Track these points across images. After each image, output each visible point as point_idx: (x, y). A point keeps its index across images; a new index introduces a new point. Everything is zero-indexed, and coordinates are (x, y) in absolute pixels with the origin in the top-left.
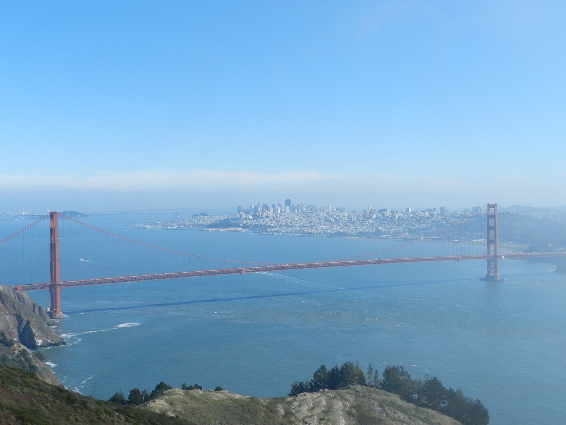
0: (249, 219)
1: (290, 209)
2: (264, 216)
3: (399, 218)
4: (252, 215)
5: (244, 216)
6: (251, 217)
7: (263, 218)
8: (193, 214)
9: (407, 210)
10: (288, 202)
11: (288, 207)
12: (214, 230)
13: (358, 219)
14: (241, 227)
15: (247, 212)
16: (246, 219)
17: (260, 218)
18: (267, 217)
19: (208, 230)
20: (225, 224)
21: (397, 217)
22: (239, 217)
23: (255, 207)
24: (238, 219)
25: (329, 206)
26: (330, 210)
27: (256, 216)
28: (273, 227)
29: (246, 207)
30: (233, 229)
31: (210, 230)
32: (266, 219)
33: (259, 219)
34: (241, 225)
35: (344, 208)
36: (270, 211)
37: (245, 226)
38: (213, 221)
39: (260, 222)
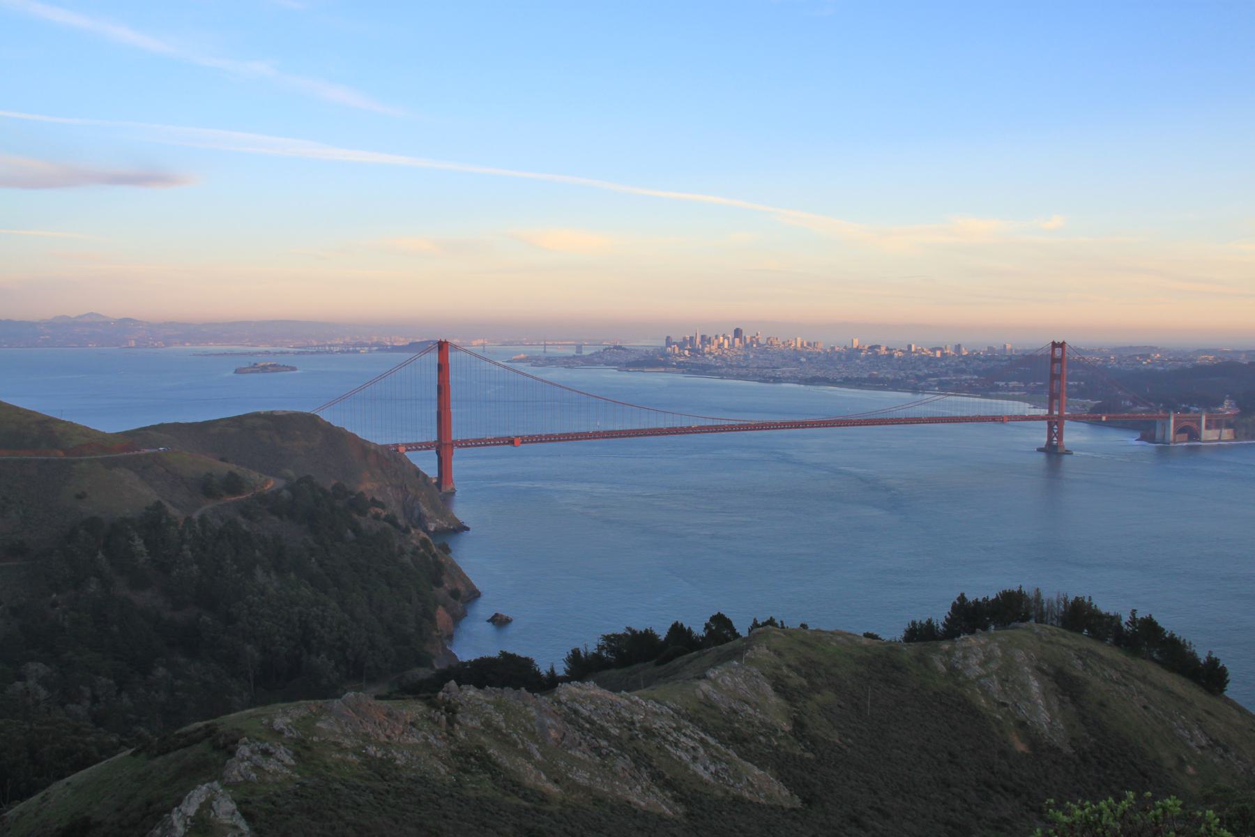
0: (685, 355)
1: (741, 342)
2: (705, 352)
4: (689, 350)
5: (677, 351)
6: (687, 352)
9: (910, 347)
10: (738, 333)
11: (737, 340)
14: (674, 366)
15: (681, 346)
16: (680, 356)
23: (691, 338)
25: (796, 339)
26: (799, 345)
29: (677, 338)
34: (675, 364)
35: (818, 343)
36: (713, 345)
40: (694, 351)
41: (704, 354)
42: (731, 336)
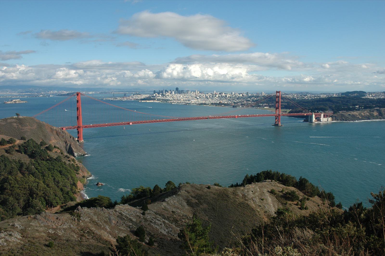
3: (229, 97)
4: (161, 95)
6: (160, 95)
7: (166, 96)
12: (144, 101)
13: (210, 97)
14: (156, 100)
16: (158, 97)
17: (165, 96)
18: (168, 96)
19: (141, 102)
21: (228, 96)
22: (155, 95)
24: (154, 96)
27: (163, 95)
28: (171, 100)
29: (157, 90)
30: (152, 101)
31: (142, 101)
32: (167, 96)
33: (164, 97)
34: (156, 99)
37: (158, 100)
38: (143, 97)
39: (164, 98)
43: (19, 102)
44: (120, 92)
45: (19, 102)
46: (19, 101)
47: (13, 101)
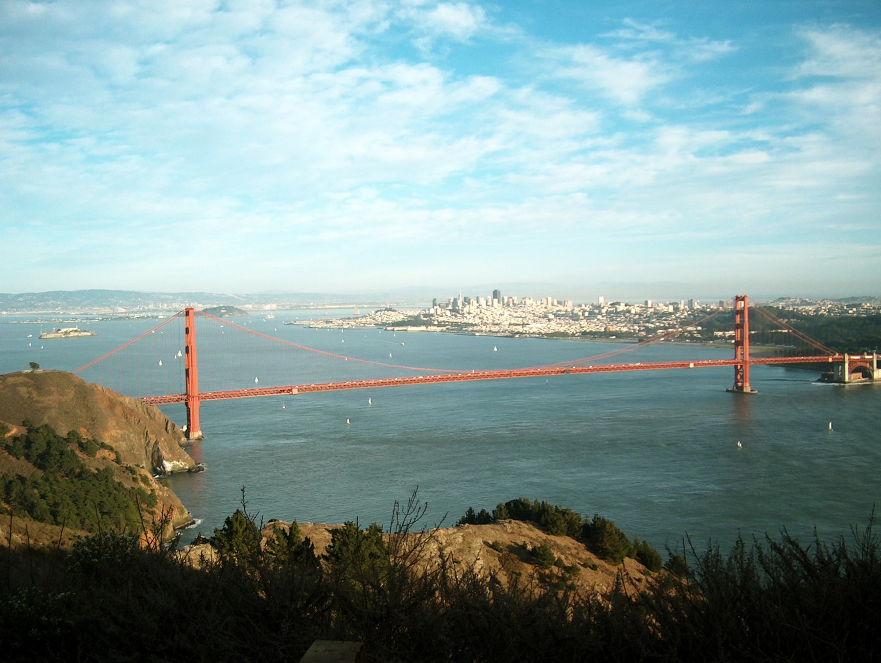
1: (499, 302)
4: (450, 310)
5: (439, 312)
6: (448, 313)
7: (463, 314)
8: (376, 310)
9: (646, 303)
10: (496, 294)
11: (496, 301)
14: (435, 325)
16: (442, 316)
17: (459, 314)
18: (469, 313)
20: (415, 321)
24: (432, 315)
27: (455, 311)
28: (475, 325)
30: (423, 328)
32: (466, 315)
33: (459, 315)
34: (436, 323)
37: (439, 325)
38: (400, 318)
39: (459, 320)
40: (455, 311)
41: (464, 314)
42: (490, 298)
43: (76, 334)
44: (345, 304)
45: (76, 334)
46: (76, 331)
47: (62, 333)
